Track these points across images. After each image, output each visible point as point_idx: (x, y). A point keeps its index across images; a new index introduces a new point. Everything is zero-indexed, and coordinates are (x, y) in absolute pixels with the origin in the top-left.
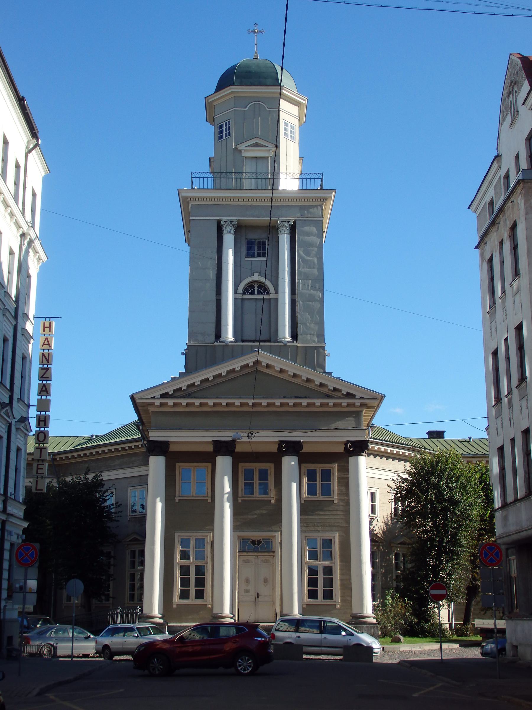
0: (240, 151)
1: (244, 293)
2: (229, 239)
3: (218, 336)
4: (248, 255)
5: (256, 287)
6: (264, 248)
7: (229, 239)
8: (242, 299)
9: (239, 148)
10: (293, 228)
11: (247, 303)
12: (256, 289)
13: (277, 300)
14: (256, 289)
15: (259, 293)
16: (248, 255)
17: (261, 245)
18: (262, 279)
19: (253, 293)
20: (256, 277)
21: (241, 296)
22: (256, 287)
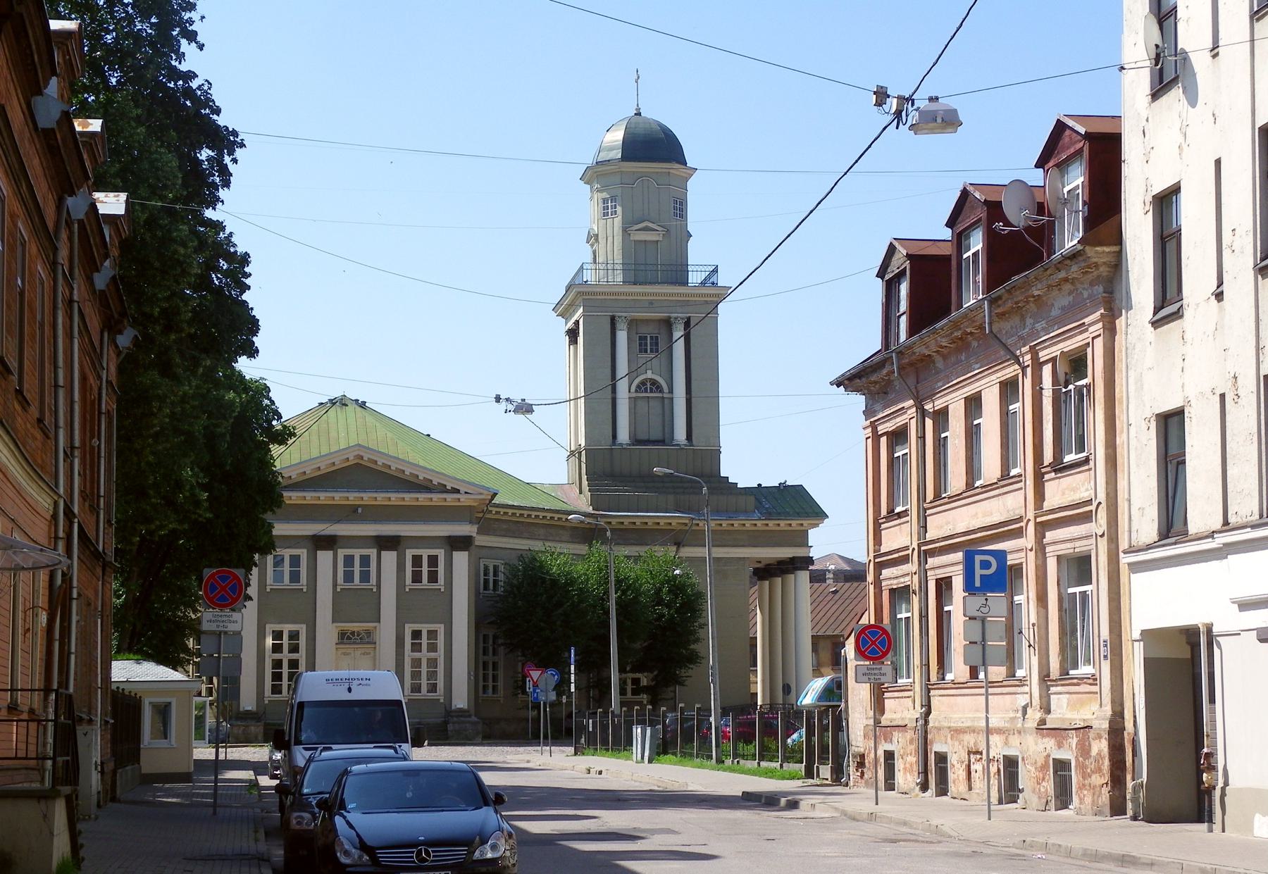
0: (630, 234)
1: (636, 391)
2: (622, 336)
3: (614, 436)
4: (640, 351)
5: (648, 384)
6: (657, 344)
7: (622, 336)
8: (635, 398)
9: (629, 232)
10: (687, 324)
11: (641, 404)
12: (649, 386)
13: (672, 399)
14: (649, 386)
15: (651, 392)
16: (640, 351)
17: (655, 341)
18: (654, 377)
19: (646, 391)
20: (649, 375)
21: (634, 395)
22: (648, 384)
